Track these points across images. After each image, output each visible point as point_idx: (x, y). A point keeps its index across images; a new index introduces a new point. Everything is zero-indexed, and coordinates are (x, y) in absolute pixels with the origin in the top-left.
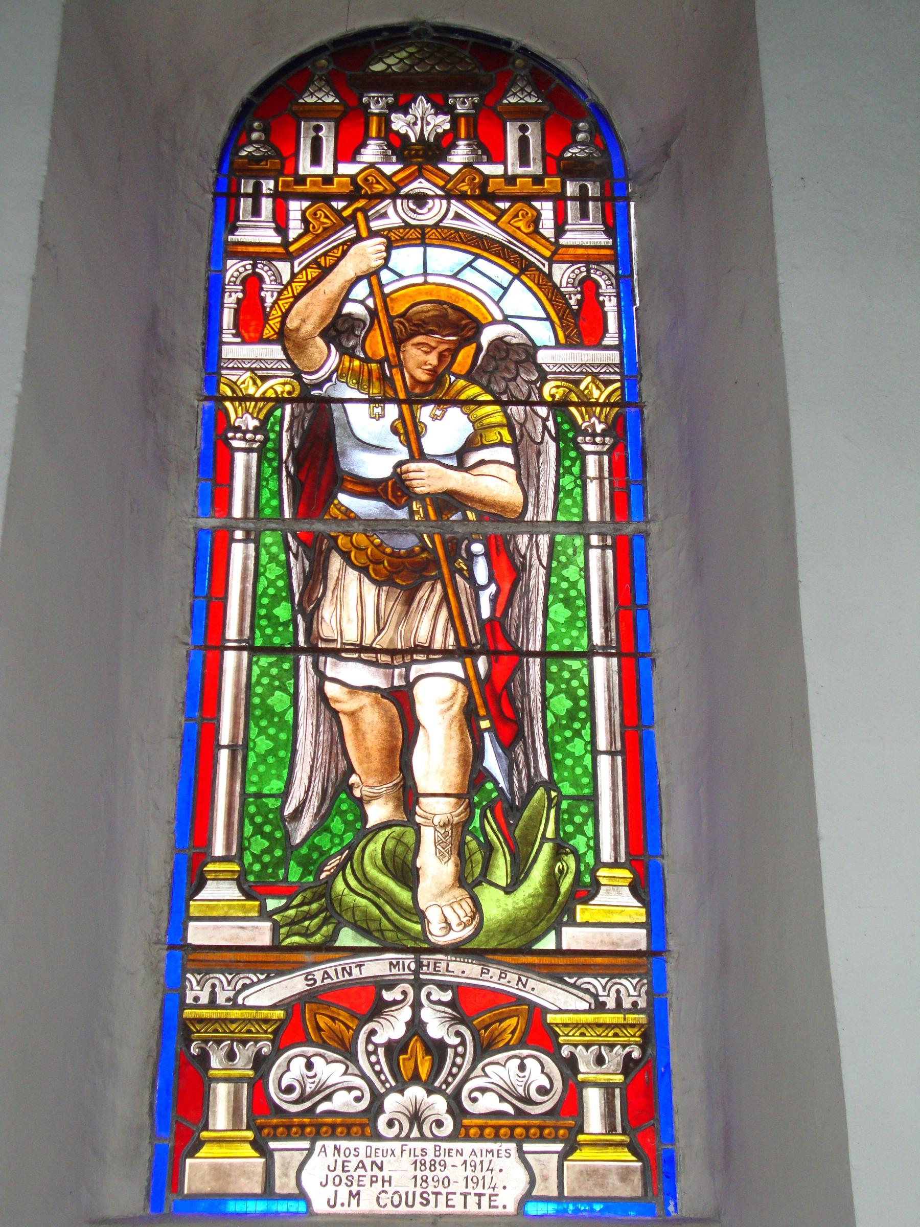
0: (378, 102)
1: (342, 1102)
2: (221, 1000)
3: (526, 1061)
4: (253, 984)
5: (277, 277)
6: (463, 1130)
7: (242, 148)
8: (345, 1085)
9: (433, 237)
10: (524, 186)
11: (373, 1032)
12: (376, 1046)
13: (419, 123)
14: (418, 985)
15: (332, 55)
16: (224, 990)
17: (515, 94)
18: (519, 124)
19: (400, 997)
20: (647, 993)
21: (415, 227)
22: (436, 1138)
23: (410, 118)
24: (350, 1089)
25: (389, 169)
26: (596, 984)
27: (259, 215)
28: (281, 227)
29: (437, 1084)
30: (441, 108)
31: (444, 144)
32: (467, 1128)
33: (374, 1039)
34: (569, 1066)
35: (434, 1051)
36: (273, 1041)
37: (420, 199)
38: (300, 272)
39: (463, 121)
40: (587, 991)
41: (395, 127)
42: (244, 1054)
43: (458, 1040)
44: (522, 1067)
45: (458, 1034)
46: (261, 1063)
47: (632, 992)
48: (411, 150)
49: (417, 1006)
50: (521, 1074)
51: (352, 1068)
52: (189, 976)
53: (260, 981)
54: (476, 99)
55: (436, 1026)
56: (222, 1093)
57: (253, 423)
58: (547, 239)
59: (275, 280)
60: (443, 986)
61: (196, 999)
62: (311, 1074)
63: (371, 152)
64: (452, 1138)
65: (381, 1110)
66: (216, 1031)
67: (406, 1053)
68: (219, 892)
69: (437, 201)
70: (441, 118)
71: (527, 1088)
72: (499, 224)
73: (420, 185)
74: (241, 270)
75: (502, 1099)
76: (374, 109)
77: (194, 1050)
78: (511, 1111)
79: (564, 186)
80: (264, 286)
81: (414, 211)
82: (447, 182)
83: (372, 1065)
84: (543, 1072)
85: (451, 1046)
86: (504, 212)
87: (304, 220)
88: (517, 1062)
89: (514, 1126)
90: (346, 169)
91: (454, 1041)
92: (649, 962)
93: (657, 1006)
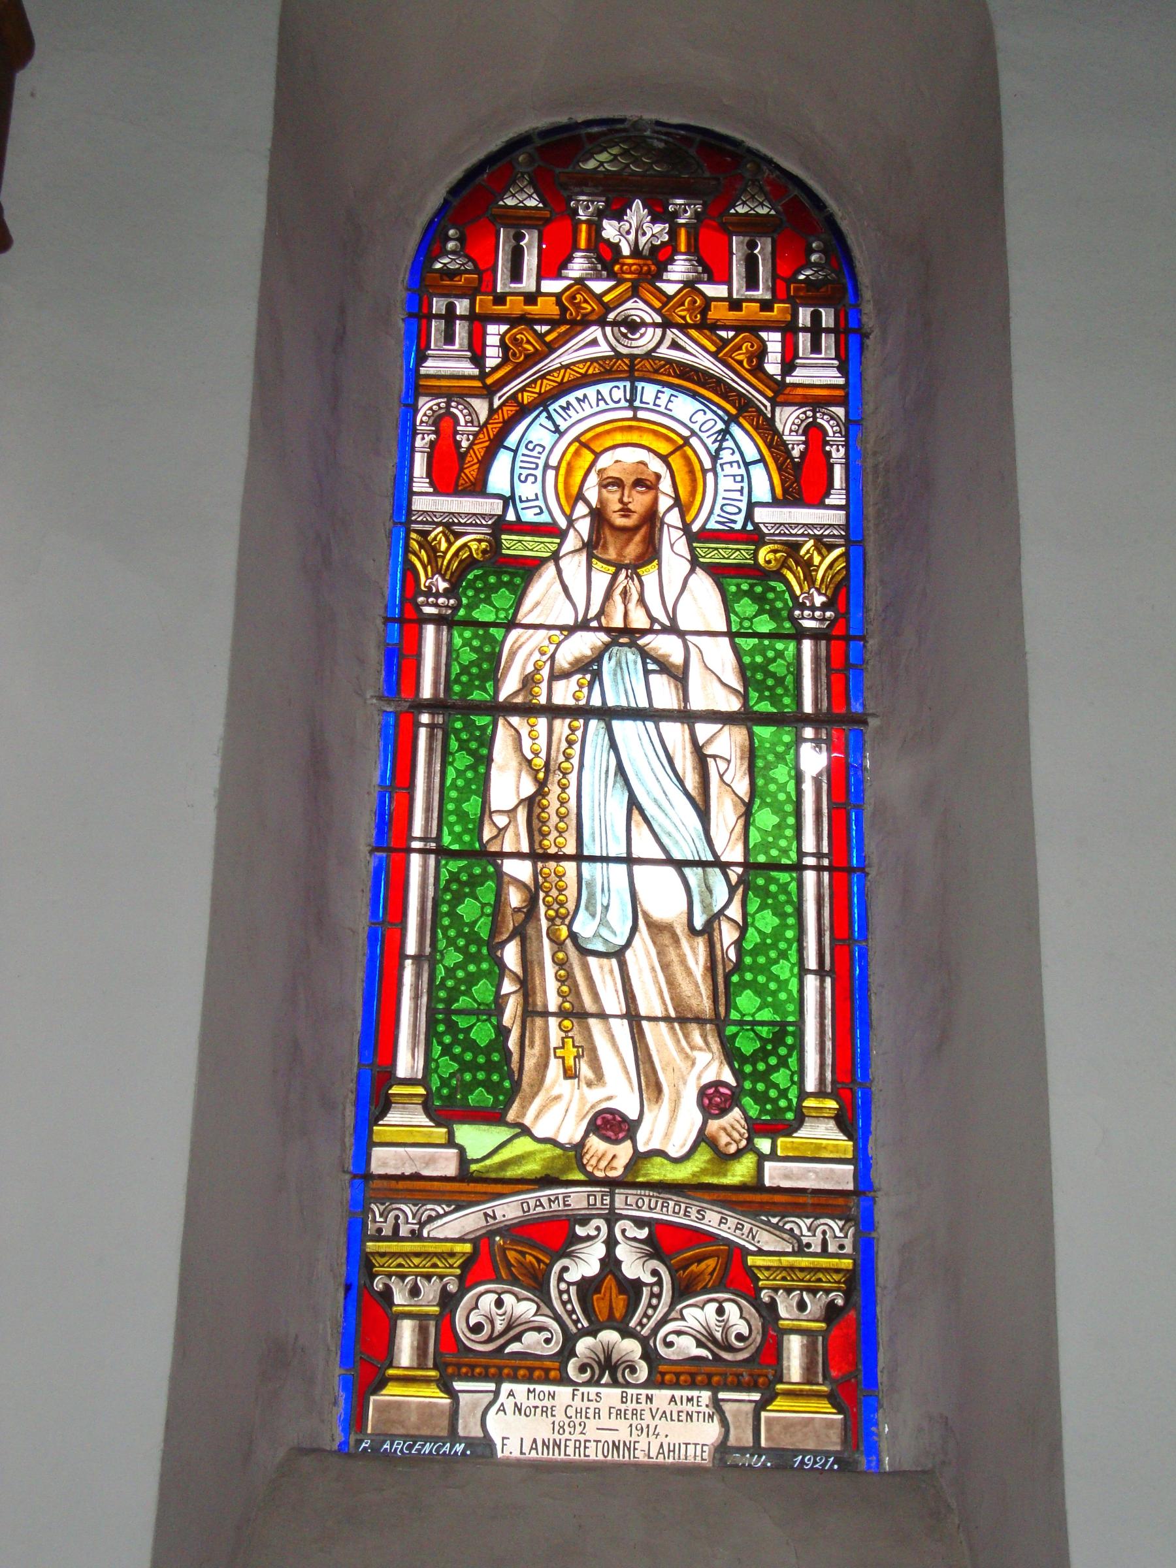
0: (588, 207)
1: (531, 1342)
2: (404, 1231)
3: (724, 1304)
4: (439, 1216)
7: (436, 259)
8: (536, 1324)
10: (750, 311)
11: (565, 1269)
12: (569, 1284)
13: (633, 231)
14: (612, 1218)
15: (539, 149)
17: (744, 203)
19: (593, 1233)
20: (854, 1235)
21: (627, 356)
24: (540, 1329)
25: (598, 287)
27: (452, 342)
28: (478, 358)
29: (632, 1324)
31: (661, 256)
32: (663, 1374)
33: (566, 1276)
34: (769, 1312)
37: (633, 326)
39: (683, 232)
42: (430, 1291)
44: (720, 1311)
45: (655, 1273)
46: (448, 1301)
48: (623, 264)
49: (611, 1243)
52: (373, 1206)
53: (446, 1214)
54: (699, 208)
55: (633, 1266)
56: (406, 1332)
57: (443, 585)
58: (771, 377)
59: (472, 422)
60: (639, 1223)
61: (380, 1230)
62: (501, 1312)
63: (578, 267)
64: (646, 1385)
66: (400, 1266)
67: (599, 1292)
69: (650, 330)
70: (657, 228)
74: (435, 408)
75: (700, 1344)
76: (582, 215)
77: (378, 1285)
79: (795, 315)
82: (665, 305)
83: (564, 1304)
84: (741, 1317)
85: (646, 1285)
87: (503, 345)
88: (716, 1305)
90: (552, 286)
91: (648, 1278)
93: (866, 1249)
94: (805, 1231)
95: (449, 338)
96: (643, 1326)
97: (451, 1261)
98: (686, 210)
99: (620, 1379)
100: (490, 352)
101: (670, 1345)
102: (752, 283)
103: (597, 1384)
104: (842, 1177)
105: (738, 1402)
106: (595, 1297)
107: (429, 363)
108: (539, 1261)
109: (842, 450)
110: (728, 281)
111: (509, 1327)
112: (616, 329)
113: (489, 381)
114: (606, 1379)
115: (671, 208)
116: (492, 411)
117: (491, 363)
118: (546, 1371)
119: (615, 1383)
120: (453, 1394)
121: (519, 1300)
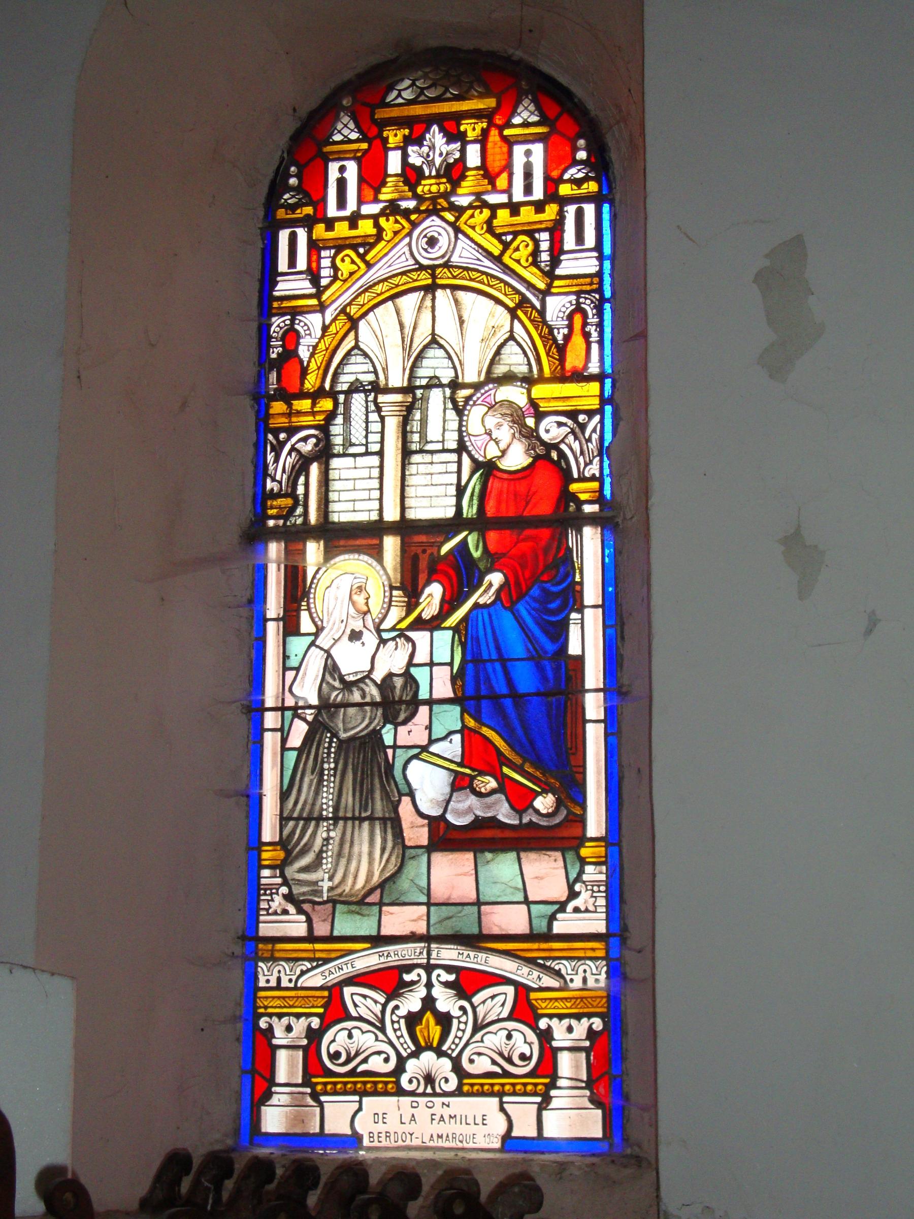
0: (396, 135)
2: (285, 983)
3: (512, 1033)
4: (308, 970)
14: (429, 968)
19: (416, 978)
23: (425, 149)
24: (379, 1053)
29: (444, 1048)
31: (455, 175)
38: (331, 324)
43: (461, 1013)
44: (509, 1037)
45: (462, 1008)
49: (429, 985)
50: (507, 1042)
51: (381, 1036)
55: (446, 1001)
60: (449, 969)
65: (404, 1071)
73: (433, 224)
75: (494, 1062)
81: (425, 250)
84: (525, 1042)
88: (506, 1032)
94: (570, 972)
96: (453, 1050)
99: (438, 1090)
100: (325, 273)
103: (424, 1094)
110: (508, 191)
111: (357, 1054)
115: (462, 128)
117: (324, 282)
120: (321, 1105)
121: (363, 1033)
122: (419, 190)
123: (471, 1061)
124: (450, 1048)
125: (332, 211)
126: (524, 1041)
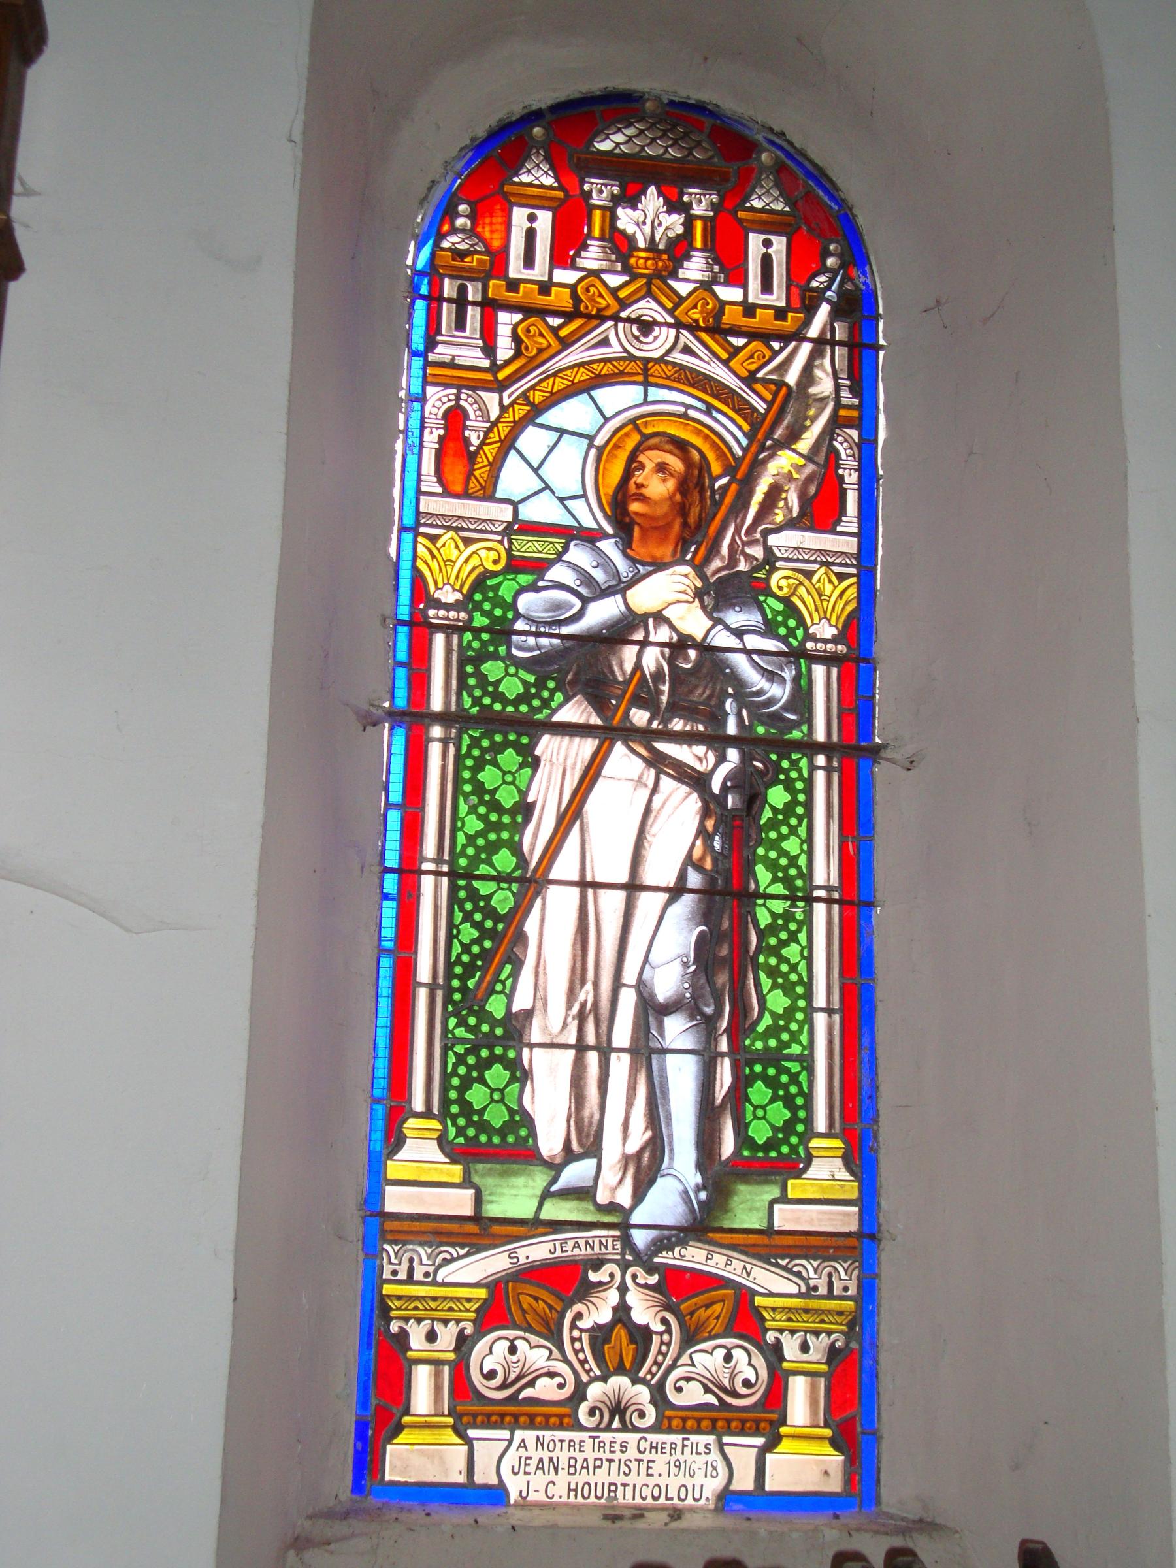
0: (601, 192)
2: (418, 1275)
4: (453, 1260)
5: (484, 414)
6: (666, 1422)
9: (656, 374)
11: (579, 1316)
12: (581, 1330)
13: (648, 222)
15: (550, 123)
16: (421, 1264)
18: (763, 237)
19: (606, 1279)
22: (636, 1429)
24: (552, 1375)
26: (808, 1267)
27: (464, 330)
28: (489, 348)
29: (641, 1374)
30: (673, 206)
32: (670, 1419)
33: (579, 1324)
35: (639, 1339)
36: (474, 1321)
37: (646, 327)
39: (699, 225)
40: (798, 1274)
41: (621, 224)
42: (447, 1337)
44: (728, 1358)
45: (664, 1321)
46: (463, 1343)
47: (843, 1276)
49: (623, 1289)
53: (460, 1257)
55: (643, 1312)
56: (422, 1377)
63: (592, 257)
66: (416, 1308)
68: (420, 1151)
69: (664, 329)
70: (675, 217)
71: (732, 1378)
72: (731, 364)
73: (647, 305)
74: (445, 399)
75: (707, 1390)
76: (596, 200)
77: (394, 1327)
78: (716, 1402)
80: (468, 423)
81: (637, 338)
82: (677, 306)
84: (750, 1364)
85: (657, 1333)
86: (738, 350)
87: (515, 337)
88: (723, 1351)
89: (718, 1419)
90: (564, 276)
92: (861, 1245)
93: (868, 1289)
95: (460, 324)
97: (468, 1305)
98: (701, 203)
101: (679, 1390)
102: (767, 287)
103: (608, 1428)
104: (845, 1219)
105: (743, 1450)
106: (606, 1347)
107: (440, 349)
108: (551, 1307)
109: (855, 475)
112: (628, 325)
113: (501, 376)
114: (616, 1424)
116: (503, 409)
118: (559, 1416)
119: (624, 1428)
120: (469, 1442)
122: (633, 261)
123: (679, 1390)
124: (650, 1372)
125: (515, 269)
126: (748, 1366)
